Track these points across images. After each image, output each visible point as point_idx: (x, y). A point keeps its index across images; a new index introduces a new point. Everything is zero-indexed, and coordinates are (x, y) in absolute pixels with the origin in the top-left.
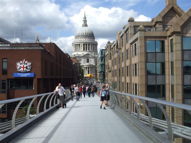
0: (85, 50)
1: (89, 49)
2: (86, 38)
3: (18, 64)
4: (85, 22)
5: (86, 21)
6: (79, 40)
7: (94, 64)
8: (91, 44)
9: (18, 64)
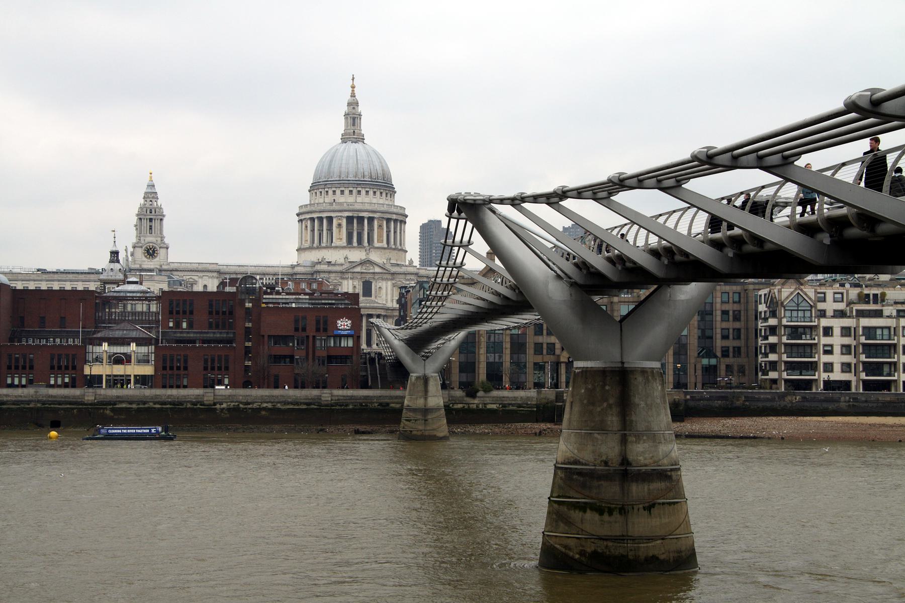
0: (355, 243)
1: (370, 240)
2: (359, 192)
3: (339, 322)
4: (354, 119)
5: (360, 115)
6: (329, 198)
7: (392, 300)
9: (339, 322)
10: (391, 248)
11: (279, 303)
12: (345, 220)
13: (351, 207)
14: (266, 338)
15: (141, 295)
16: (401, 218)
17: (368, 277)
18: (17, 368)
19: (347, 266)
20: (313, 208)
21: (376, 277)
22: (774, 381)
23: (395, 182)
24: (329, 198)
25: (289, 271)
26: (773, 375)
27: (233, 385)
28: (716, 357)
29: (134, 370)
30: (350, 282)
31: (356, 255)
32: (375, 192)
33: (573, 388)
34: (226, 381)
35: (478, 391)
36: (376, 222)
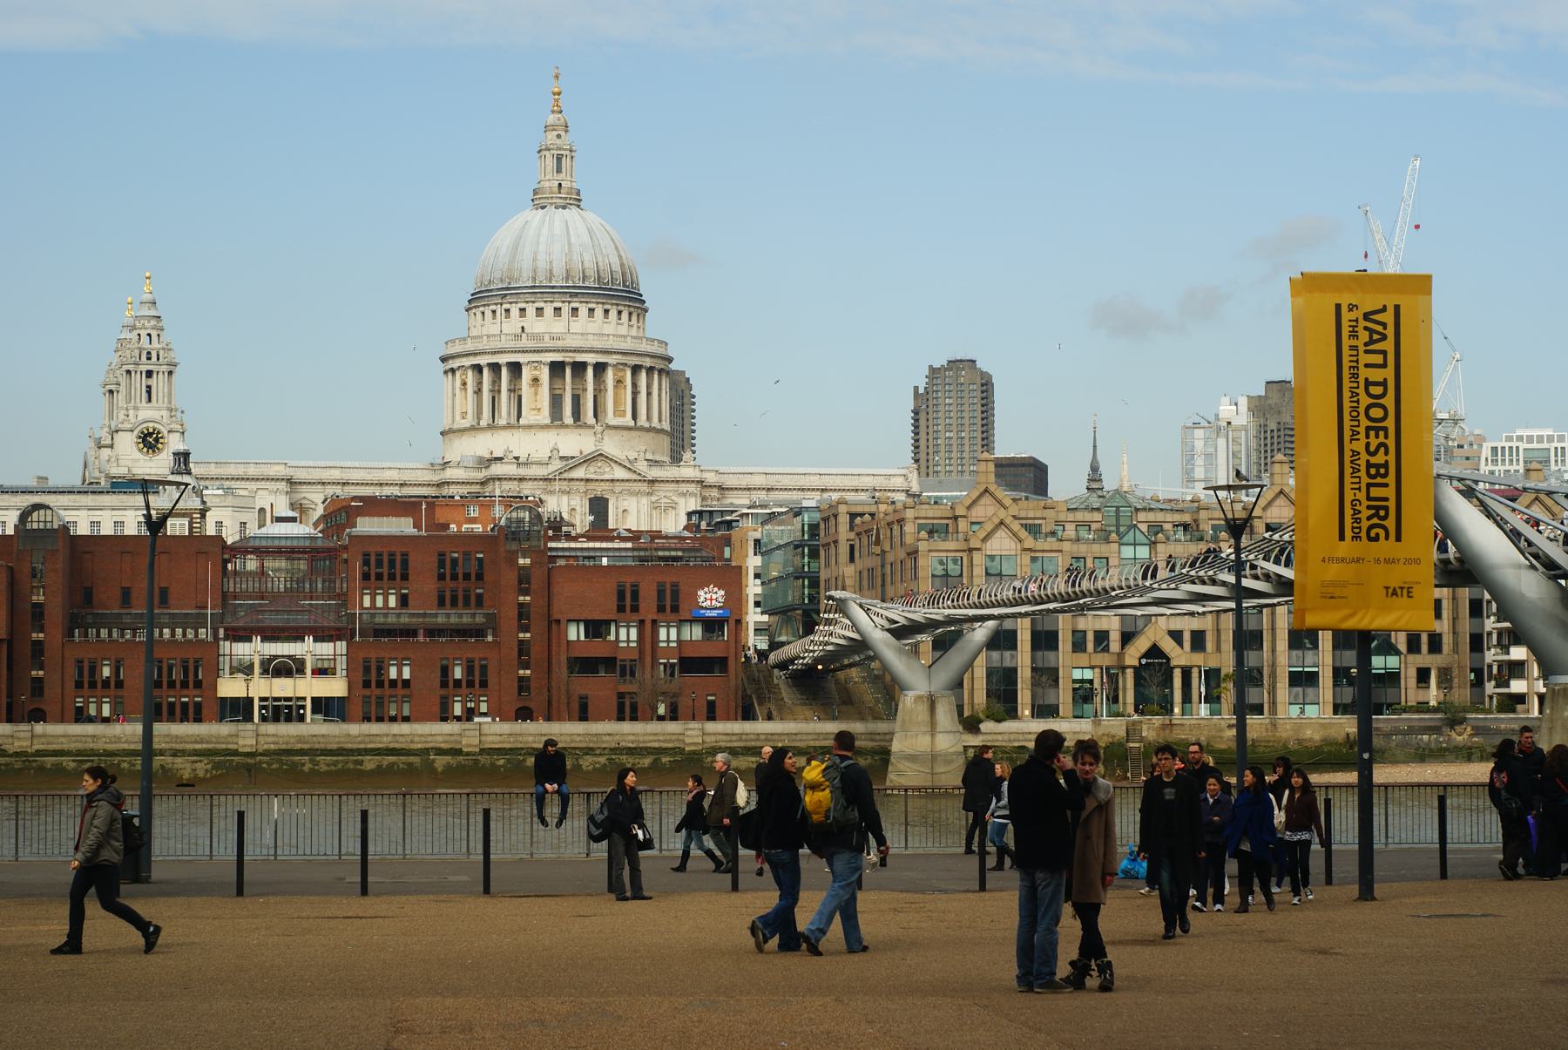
0: (568, 418)
2: (575, 310)
3: (701, 593)
4: (559, 158)
8: (619, 366)
9: (701, 593)
10: (642, 429)
11: (576, 557)
12: (546, 371)
13: (560, 344)
14: (563, 623)
15: (307, 543)
16: (659, 364)
17: (598, 490)
18: (93, 685)
19: (557, 465)
20: (480, 347)
21: (618, 487)
22: (1521, 698)
23: (645, 291)
24: (513, 324)
25: (436, 478)
26: (1518, 686)
27: (496, 712)
28: (1398, 653)
29: (308, 687)
30: (565, 498)
31: (574, 443)
32: (606, 311)
33: (1552, 709)
34: (484, 708)
35: (981, 721)
36: (610, 373)
